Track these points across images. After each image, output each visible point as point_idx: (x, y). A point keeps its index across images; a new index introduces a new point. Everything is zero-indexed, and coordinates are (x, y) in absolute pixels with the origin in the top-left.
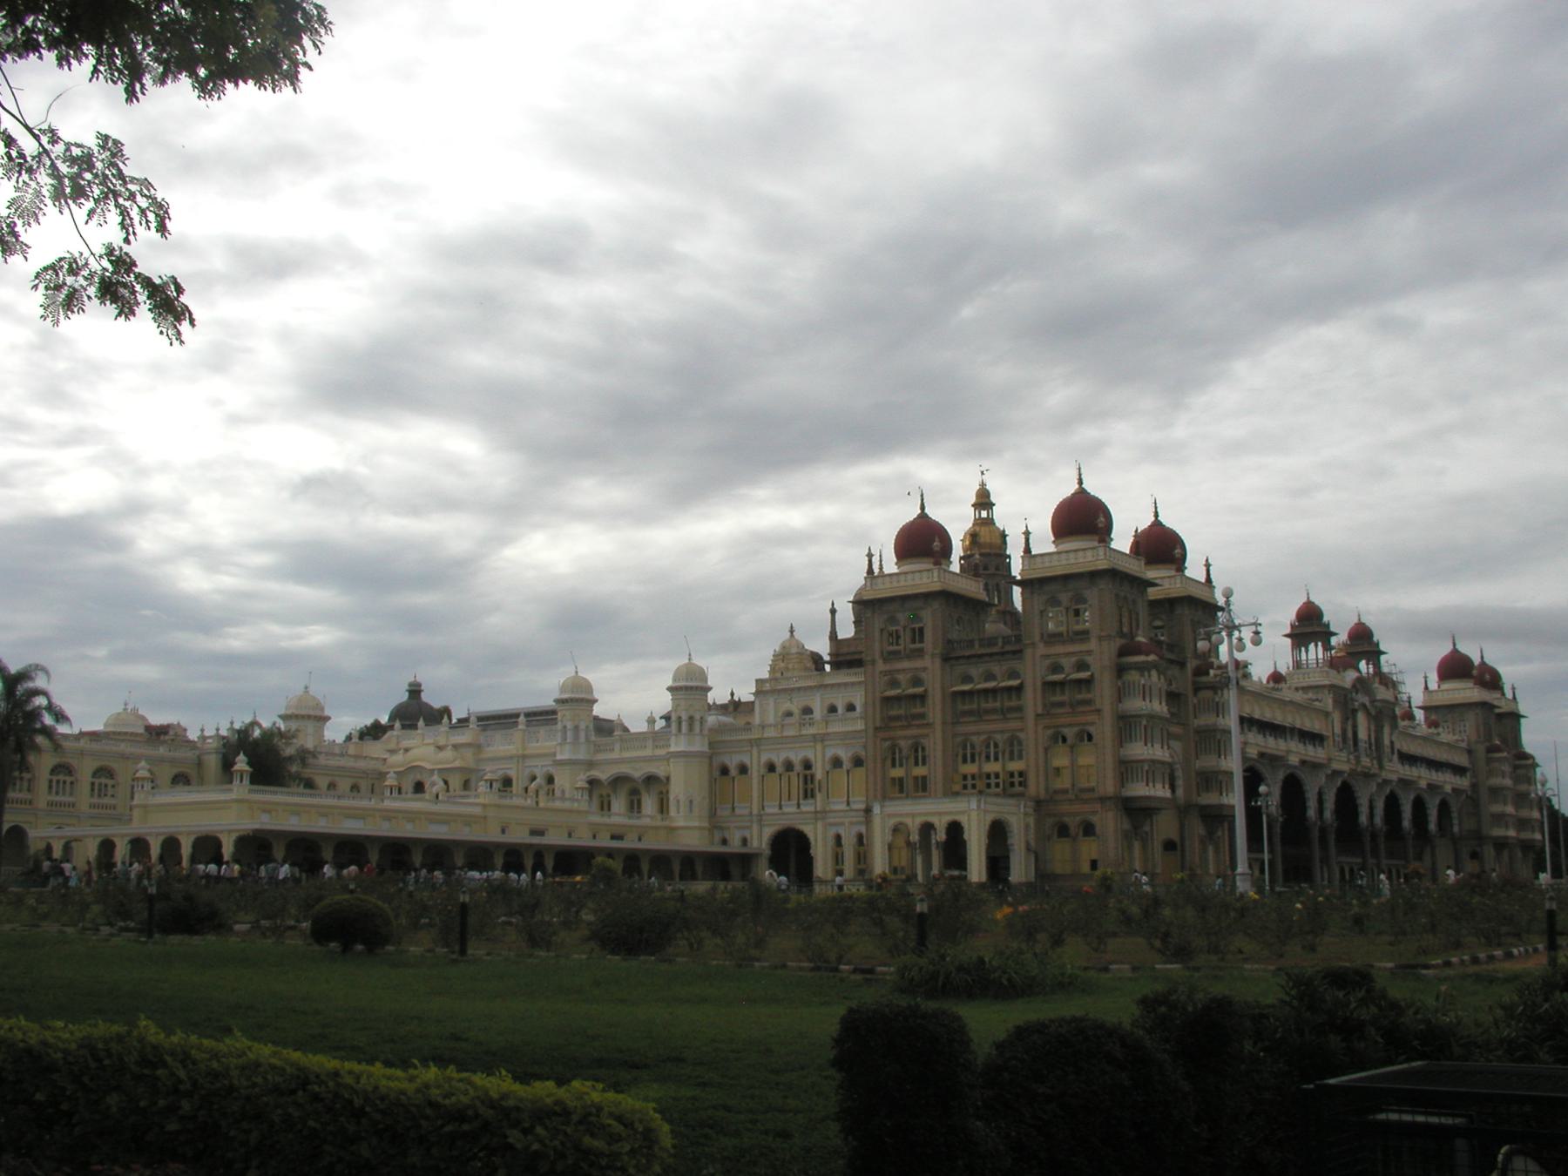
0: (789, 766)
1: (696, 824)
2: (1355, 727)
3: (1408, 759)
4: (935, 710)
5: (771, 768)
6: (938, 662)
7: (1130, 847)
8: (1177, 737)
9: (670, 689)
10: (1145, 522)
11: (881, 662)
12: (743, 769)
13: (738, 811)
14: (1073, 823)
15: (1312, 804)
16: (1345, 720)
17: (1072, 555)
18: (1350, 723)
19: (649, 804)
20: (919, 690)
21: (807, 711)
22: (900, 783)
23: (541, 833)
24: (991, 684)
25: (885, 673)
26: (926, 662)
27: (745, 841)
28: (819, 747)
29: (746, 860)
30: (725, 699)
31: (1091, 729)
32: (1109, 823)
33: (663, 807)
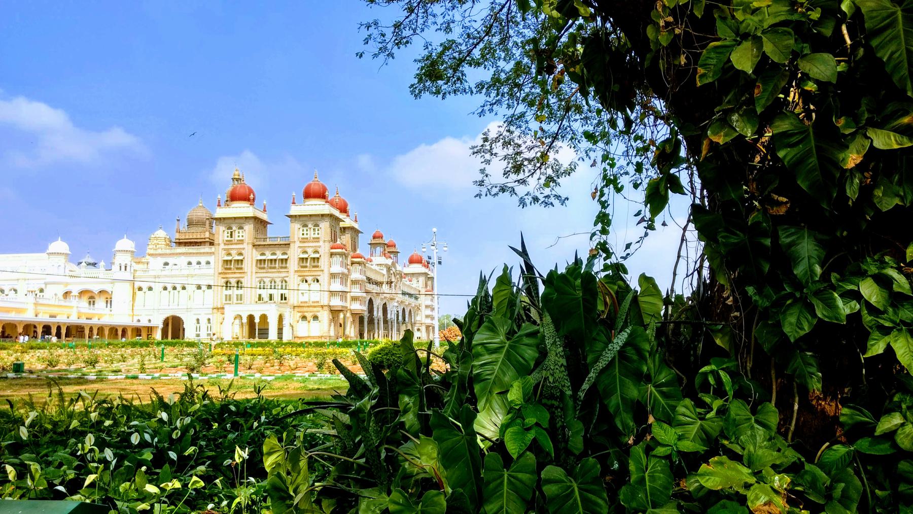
0: (175, 288)
3: (404, 294)
4: (249, 265)
6: (251, 246)
7: (330, 325)
12: (150, 289)
14: (309, 316)
15: (375, 309)
20: (240, 258)
22: (228, 298)
23: (55, 317)
24: (274, 257)
25: (225, 249)
27: (150, 321)
29: (150, 330)
32: (325, 315)
33: (109, 302)
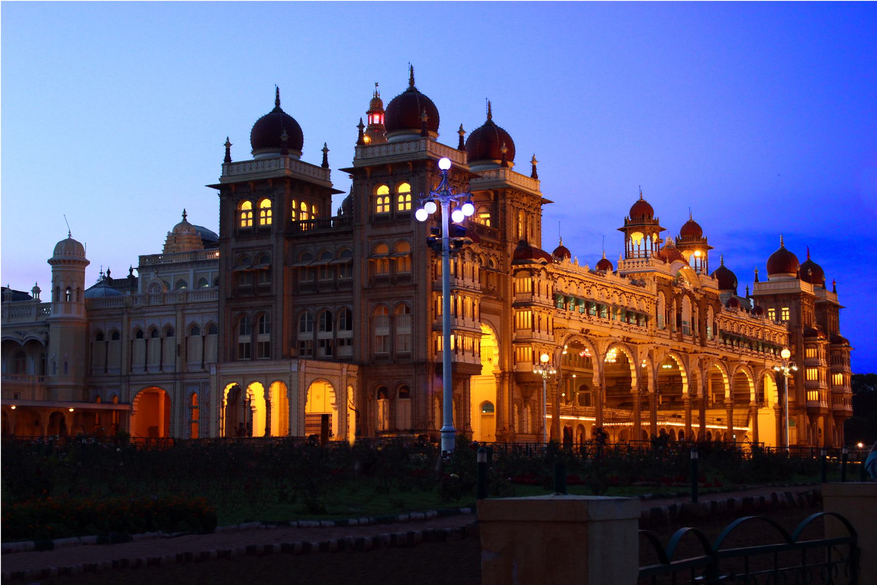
0: (154, 332)
1: (71, 383)
2: (679, 309)
5: (140, 334)
8: (496, 313)
9: (50, 261)
10: (474, 123)
11: (233, 240)
12: (116, 335)
13: (109, 372)
17: (398, 146)
19: (32, 365)
24: (325, 262)
26: (272, 240)
28: (179, 315)
30: (125, 275)
31: (409, 302)
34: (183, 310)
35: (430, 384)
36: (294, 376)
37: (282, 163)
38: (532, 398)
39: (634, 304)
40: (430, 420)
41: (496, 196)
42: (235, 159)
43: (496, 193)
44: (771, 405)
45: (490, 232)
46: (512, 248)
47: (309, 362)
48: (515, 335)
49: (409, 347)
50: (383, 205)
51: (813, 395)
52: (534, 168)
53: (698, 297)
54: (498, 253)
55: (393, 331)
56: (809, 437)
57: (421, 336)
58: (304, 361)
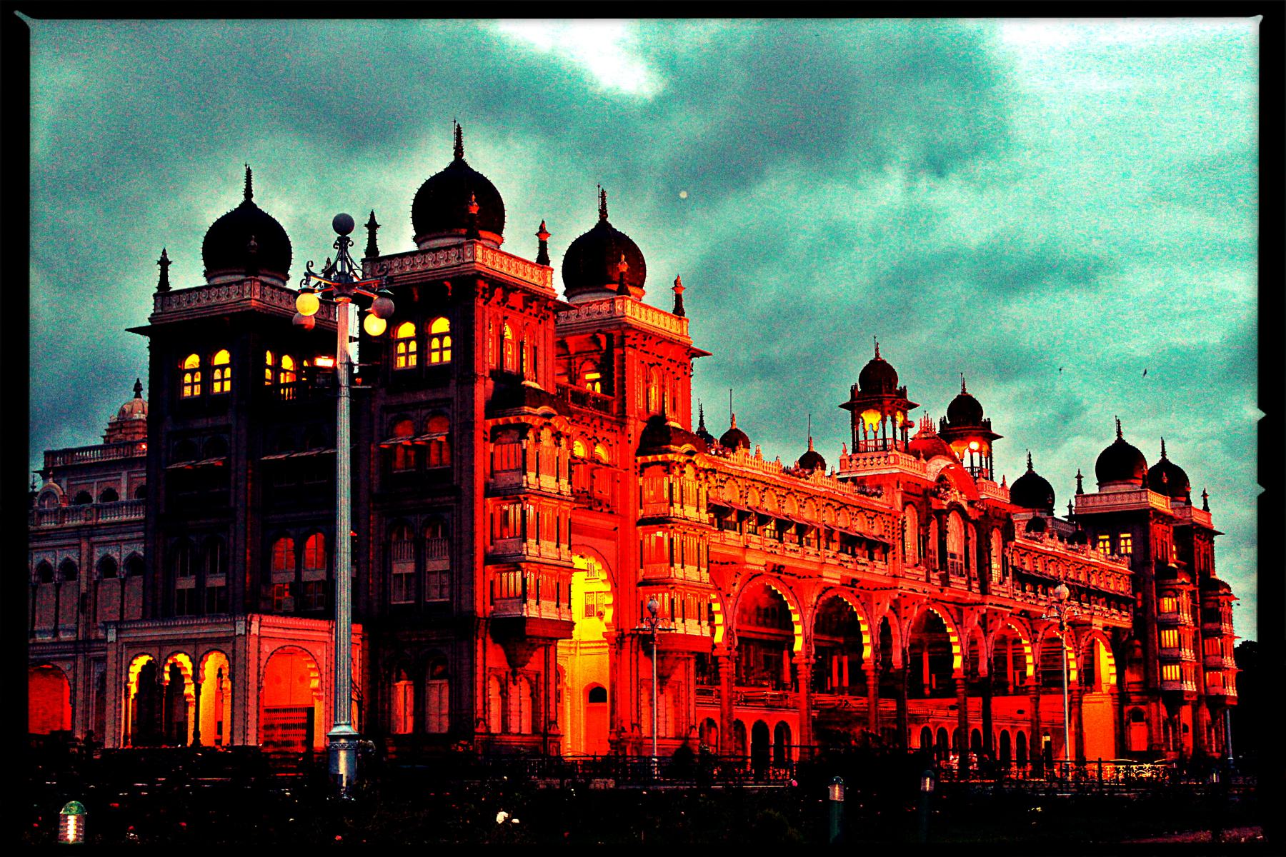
2: (943, 533)
16: (923, 524)
18: (934, 526)
21: (110, 495)
28: (85, 545)
34: (88, 537)
35: (479, 654)
36: (239, 642)
37: (247, 289)
38: (673, 678)
39: (860, 526)
40: (479, 715)
41: (610, 345)
42: (176, 284)
43: (610, 338)
44: (1105, 689)
45: (601, 404)
46: (635, 428)
47: (267, 619)
48: (642, 572)
49: (446, 591)
50: (407, 354)
51: (1171, 672)
52: (679, 299)
53: (974, 515)
54: (610, 436)
55: (420, 565)
56: (1167, 740)
57: (461, 575)
58: (256, 617)
